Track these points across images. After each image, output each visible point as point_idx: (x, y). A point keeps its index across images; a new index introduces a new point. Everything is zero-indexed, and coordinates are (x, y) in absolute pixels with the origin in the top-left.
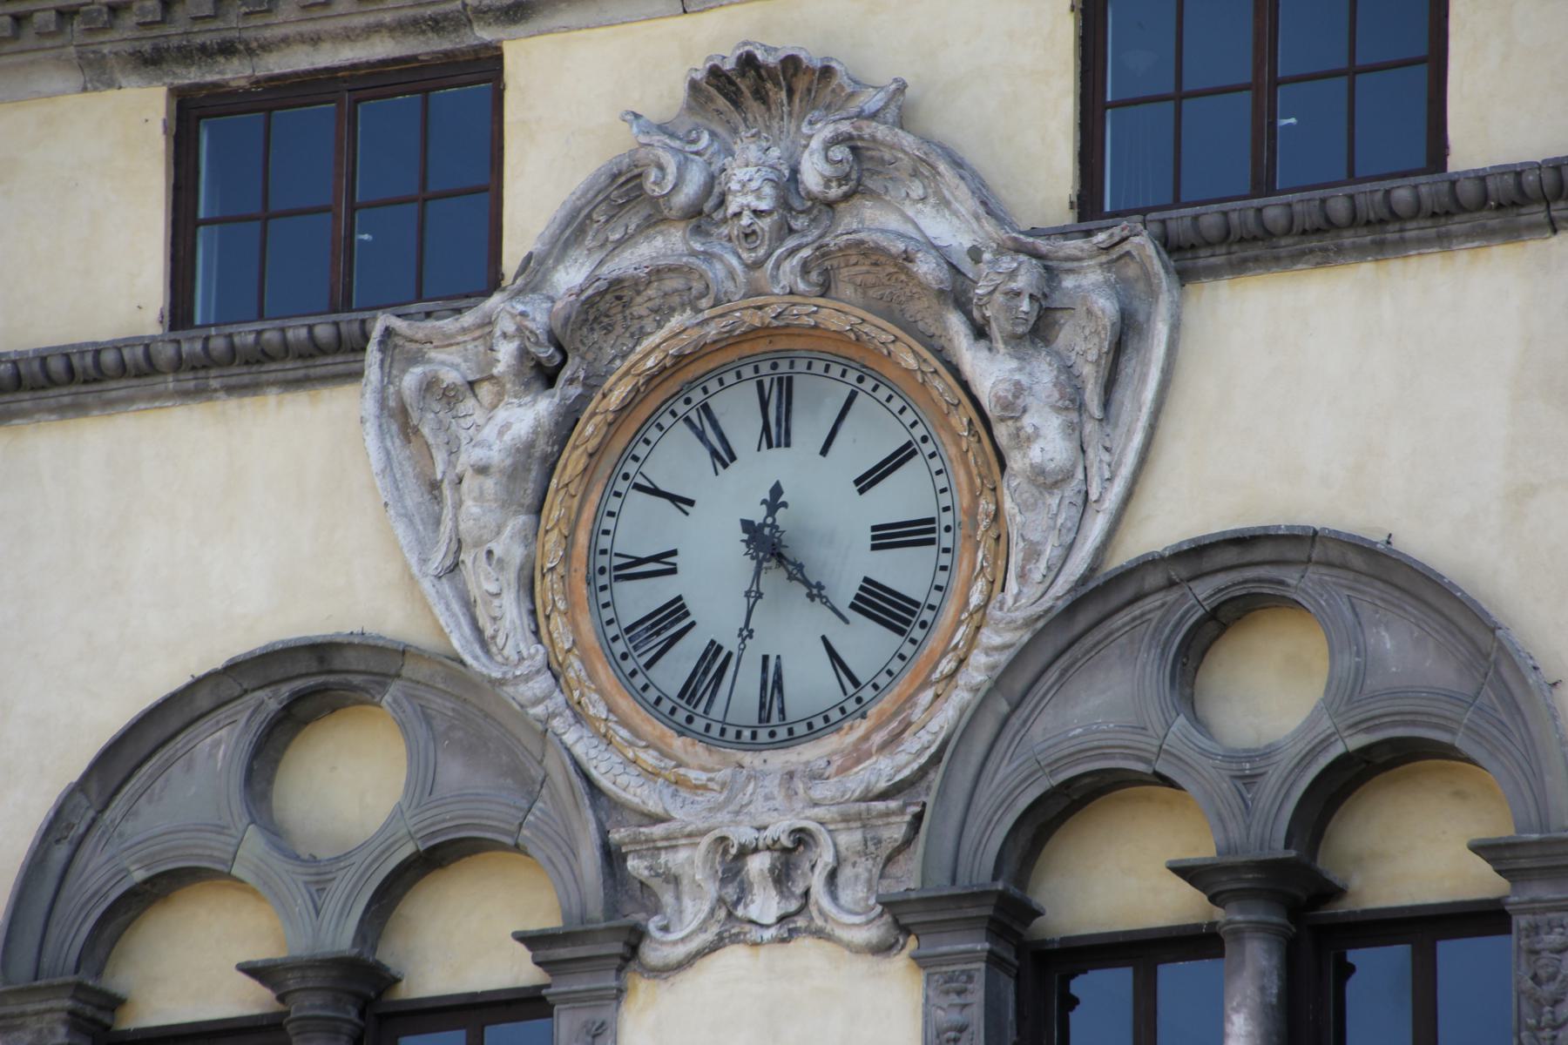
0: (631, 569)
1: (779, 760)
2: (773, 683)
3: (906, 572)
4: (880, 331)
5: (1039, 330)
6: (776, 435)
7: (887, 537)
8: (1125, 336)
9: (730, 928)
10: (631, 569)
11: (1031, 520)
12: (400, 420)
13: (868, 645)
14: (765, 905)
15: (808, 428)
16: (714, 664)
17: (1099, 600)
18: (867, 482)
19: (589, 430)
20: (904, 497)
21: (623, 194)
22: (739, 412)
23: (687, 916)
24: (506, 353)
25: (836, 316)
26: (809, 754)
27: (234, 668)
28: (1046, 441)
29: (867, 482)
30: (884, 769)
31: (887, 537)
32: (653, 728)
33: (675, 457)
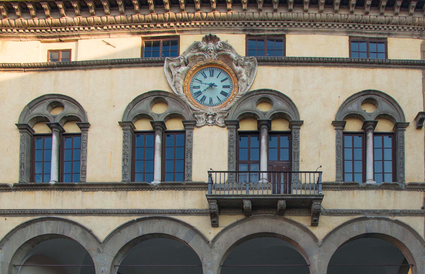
0: (195, 87)
1: (212, 108)
2: (211, 100)
3: (227, 90)
4: (225, 65)
5: (242, 66)
6: (212, 75)
7: (224, 87)
8: (252, 70)
9: (207, 124)
10: (195, 87)
11: (243, 85)
12: (169, 70)
13: (222, 97)
14: (210, 122)
15: (215, 75)
16: (204, 98)
17: (249, 95)
18: (222, 81)
19: (191, 72)
20: (227, 83)
21: (196, 46)
22: (207, 73)
23: (200, 122)
24: (182, 61)
25: (220, 62)
26: (216, 107)
27: (149, 93)
28: (244, 77)
29: (222, 81)
30: (224, 109)
31: (224, 87)
32: (197, 103)
33: (200, 77)
